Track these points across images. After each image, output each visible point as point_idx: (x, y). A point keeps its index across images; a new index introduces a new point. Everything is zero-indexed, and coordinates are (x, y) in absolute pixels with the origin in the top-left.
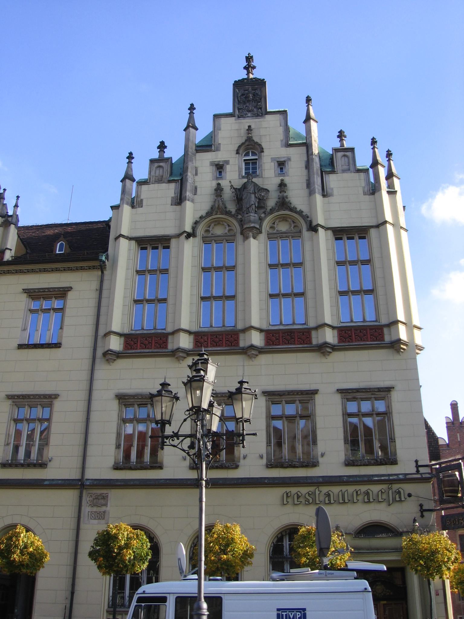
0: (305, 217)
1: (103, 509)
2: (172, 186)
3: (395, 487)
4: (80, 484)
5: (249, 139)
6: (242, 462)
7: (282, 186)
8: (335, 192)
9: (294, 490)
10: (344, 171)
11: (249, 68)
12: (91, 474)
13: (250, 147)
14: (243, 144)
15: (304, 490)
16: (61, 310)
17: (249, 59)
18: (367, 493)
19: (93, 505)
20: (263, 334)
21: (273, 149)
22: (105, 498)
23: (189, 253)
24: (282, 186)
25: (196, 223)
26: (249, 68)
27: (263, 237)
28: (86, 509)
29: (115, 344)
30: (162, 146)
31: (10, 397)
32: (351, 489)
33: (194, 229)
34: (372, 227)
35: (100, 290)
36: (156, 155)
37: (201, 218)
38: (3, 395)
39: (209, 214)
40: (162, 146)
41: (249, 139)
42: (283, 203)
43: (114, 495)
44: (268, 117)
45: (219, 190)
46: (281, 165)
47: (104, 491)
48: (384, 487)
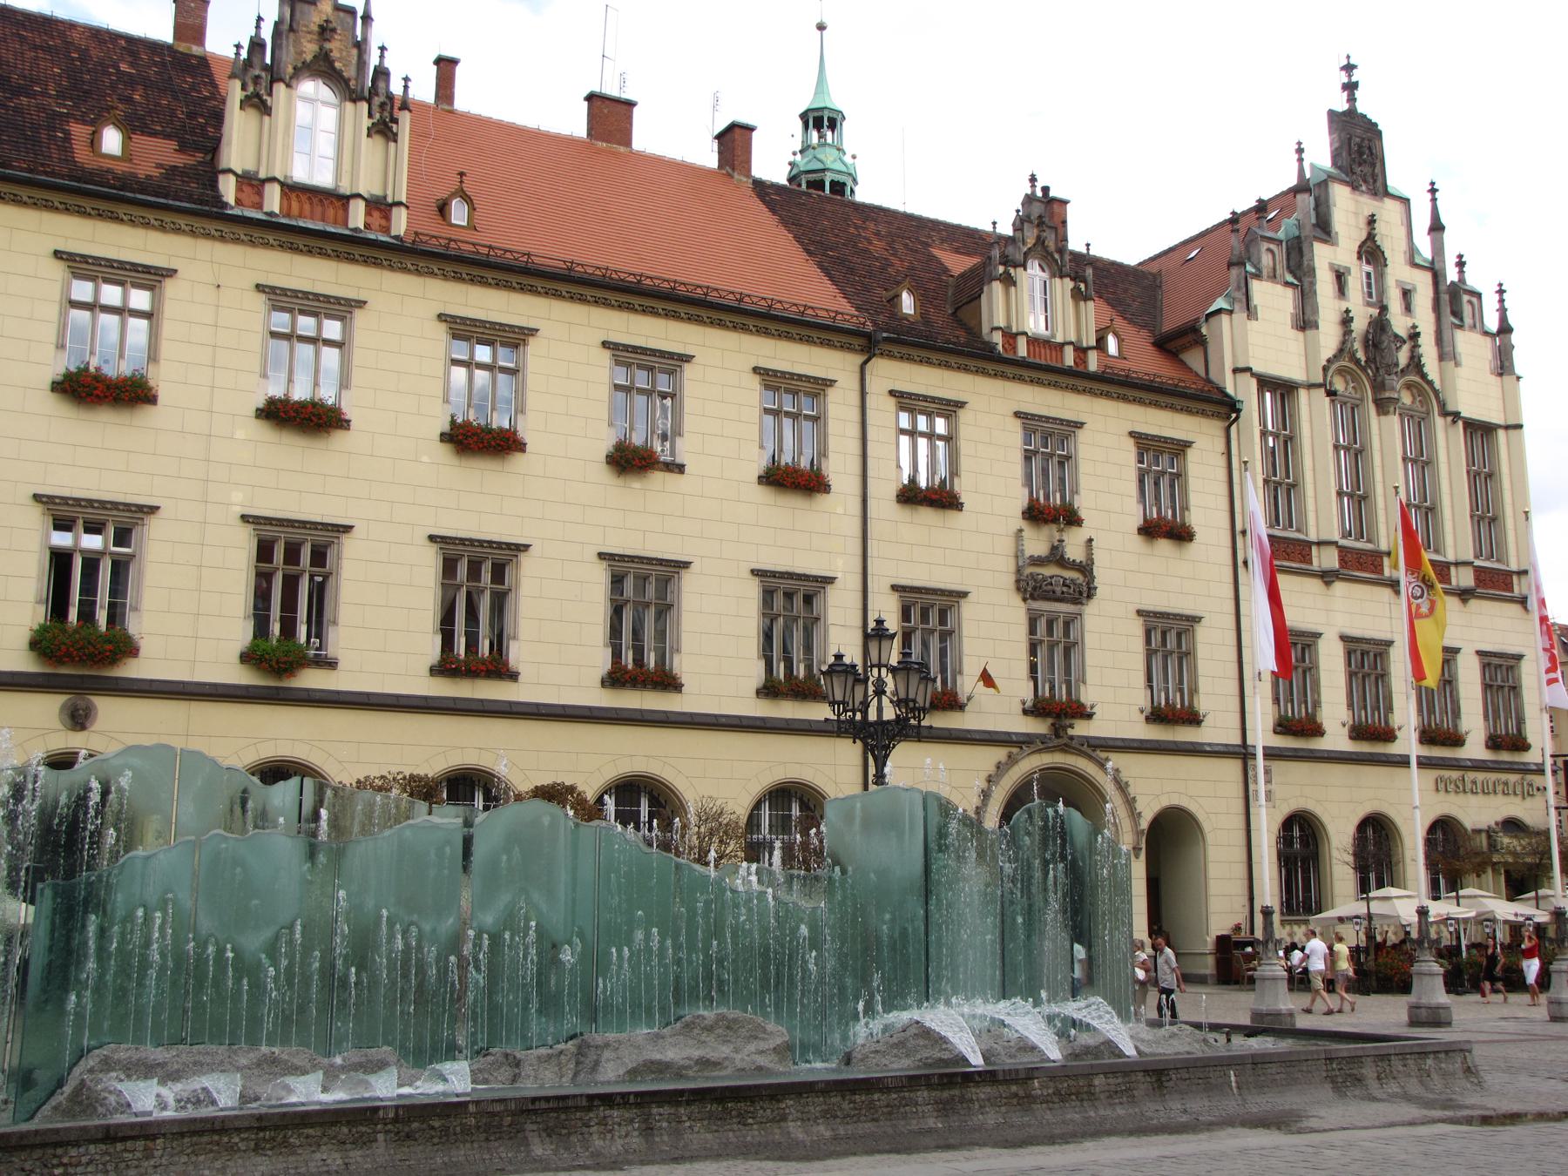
0: (1436, 393)
3: (1529, 777)
5: (1371, 237)
6: (1397, 733)
9: (1446, 773)
11: (1350, 87)
13: (1371, 251)
15: (1455, 774)
17: (1349, 68)
18: (1506, 784)
26: (1350, 87)
32: (1493, 776)
34: (1500, 426)
38: (1132, 609)
46: (1406, 294)
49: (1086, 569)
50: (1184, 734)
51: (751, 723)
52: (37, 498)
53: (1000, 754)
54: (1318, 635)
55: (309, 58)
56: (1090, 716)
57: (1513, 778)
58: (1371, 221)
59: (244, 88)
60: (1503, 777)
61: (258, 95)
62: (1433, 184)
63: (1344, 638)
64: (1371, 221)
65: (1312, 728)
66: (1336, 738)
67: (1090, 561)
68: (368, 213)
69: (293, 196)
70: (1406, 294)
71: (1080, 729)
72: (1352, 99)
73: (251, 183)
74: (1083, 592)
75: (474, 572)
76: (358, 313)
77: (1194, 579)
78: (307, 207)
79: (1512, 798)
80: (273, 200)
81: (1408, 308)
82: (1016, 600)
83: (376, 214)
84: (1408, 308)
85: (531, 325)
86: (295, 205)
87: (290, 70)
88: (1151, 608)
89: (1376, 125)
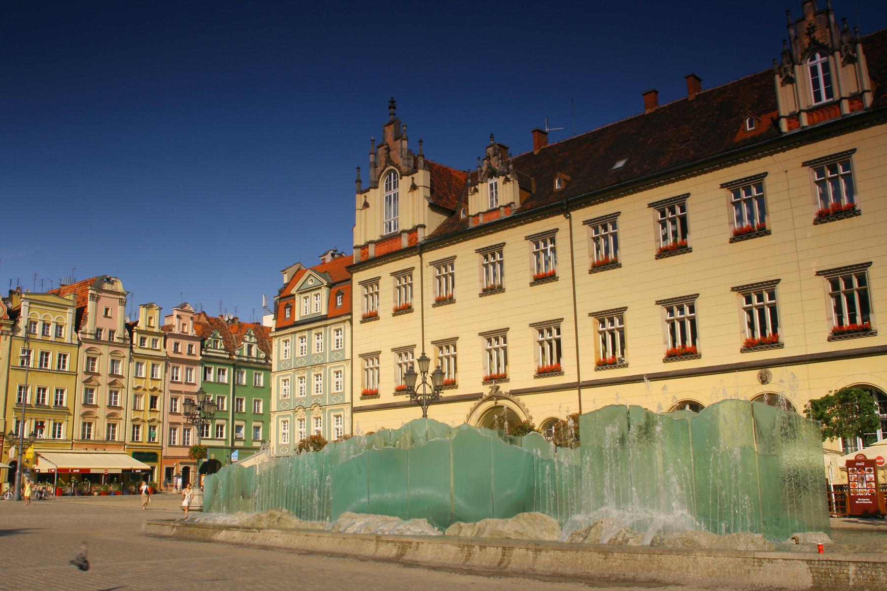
51: (812, 358)
52: (733, 289)
55: (807, 46)
59: (781, 77)
61: (788, 77)
68: (851, 104)
69: (814, 114)
73: (794, 117)
75: (849, 284)
76: (854, 156)
78: (821, 115)
80: (804, 121)
83: (856, 102)
85: (850, 148)
86: (815, 117)
87: (800, 56)
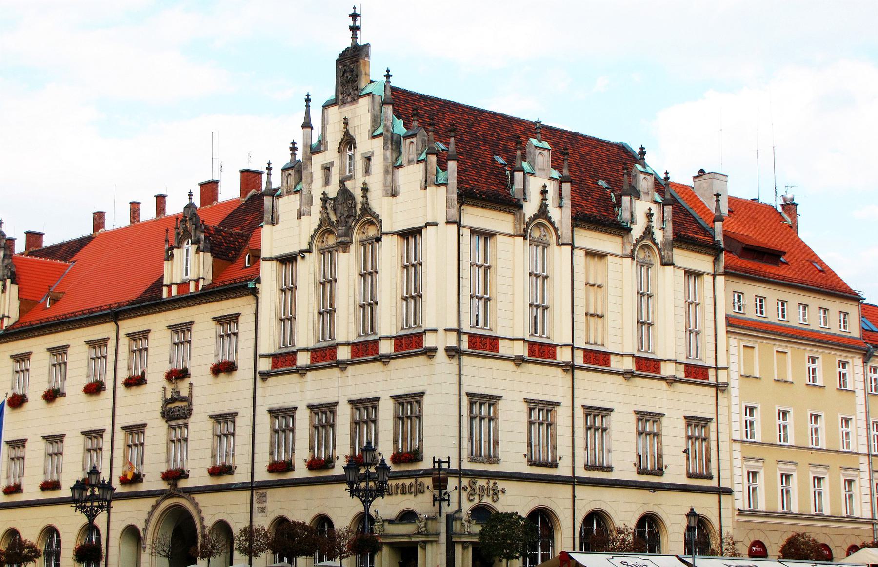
1: (265, 504)
2: (298, 195)
3: (419, 480)
4: (252, 487)
5: (347, 133)
7: (365, 190)
8: (402, 190)
10: (410, 162)
12: (257, 478)
13: (348, 142)
14: (342, 140)
16: (236, 334)
19: (259, 502)
20: (350, 347)
21: (365, 144)
22: (265, 496)
23: (307, 271)
24: (365, 190)
25: (312, 237)
27: (354, 247)
28: (256, 505)
29: (265, 365)
30: (293, 149)
31: (211, 417)
33: (310, 244)
35: (256, 314)
36: (286, 159)
37: (316, 231)
39: (320, 226)
40: (293, 149)
41: (347, 133)
42: (366, 209)
43: (270, 492)
44: (361, 101)
45: (325, 199)
47: (264, 491)
48: (413, 481)
49: (188, 400)
50: (226, 480)
53: (152, 501)
54: (296, 408)
56: (187, 477)
57: (408, 482)
58: (346, 123)
60: (400, 482)
62: (388, 71)
63: (310, 407)
64: (346, 123)
65: (288, 466)
66: (301, 471)
67: (191, 394)
70: (369, 159)
71: (183, 484)
72: (354, 37)
74: (187, 414)
77: (233, 393)
79: (408, 496)
81: (367, 171)
82: (164, 422)
84: (367, 171)
88: (216, 413)
89: (340, 55)
